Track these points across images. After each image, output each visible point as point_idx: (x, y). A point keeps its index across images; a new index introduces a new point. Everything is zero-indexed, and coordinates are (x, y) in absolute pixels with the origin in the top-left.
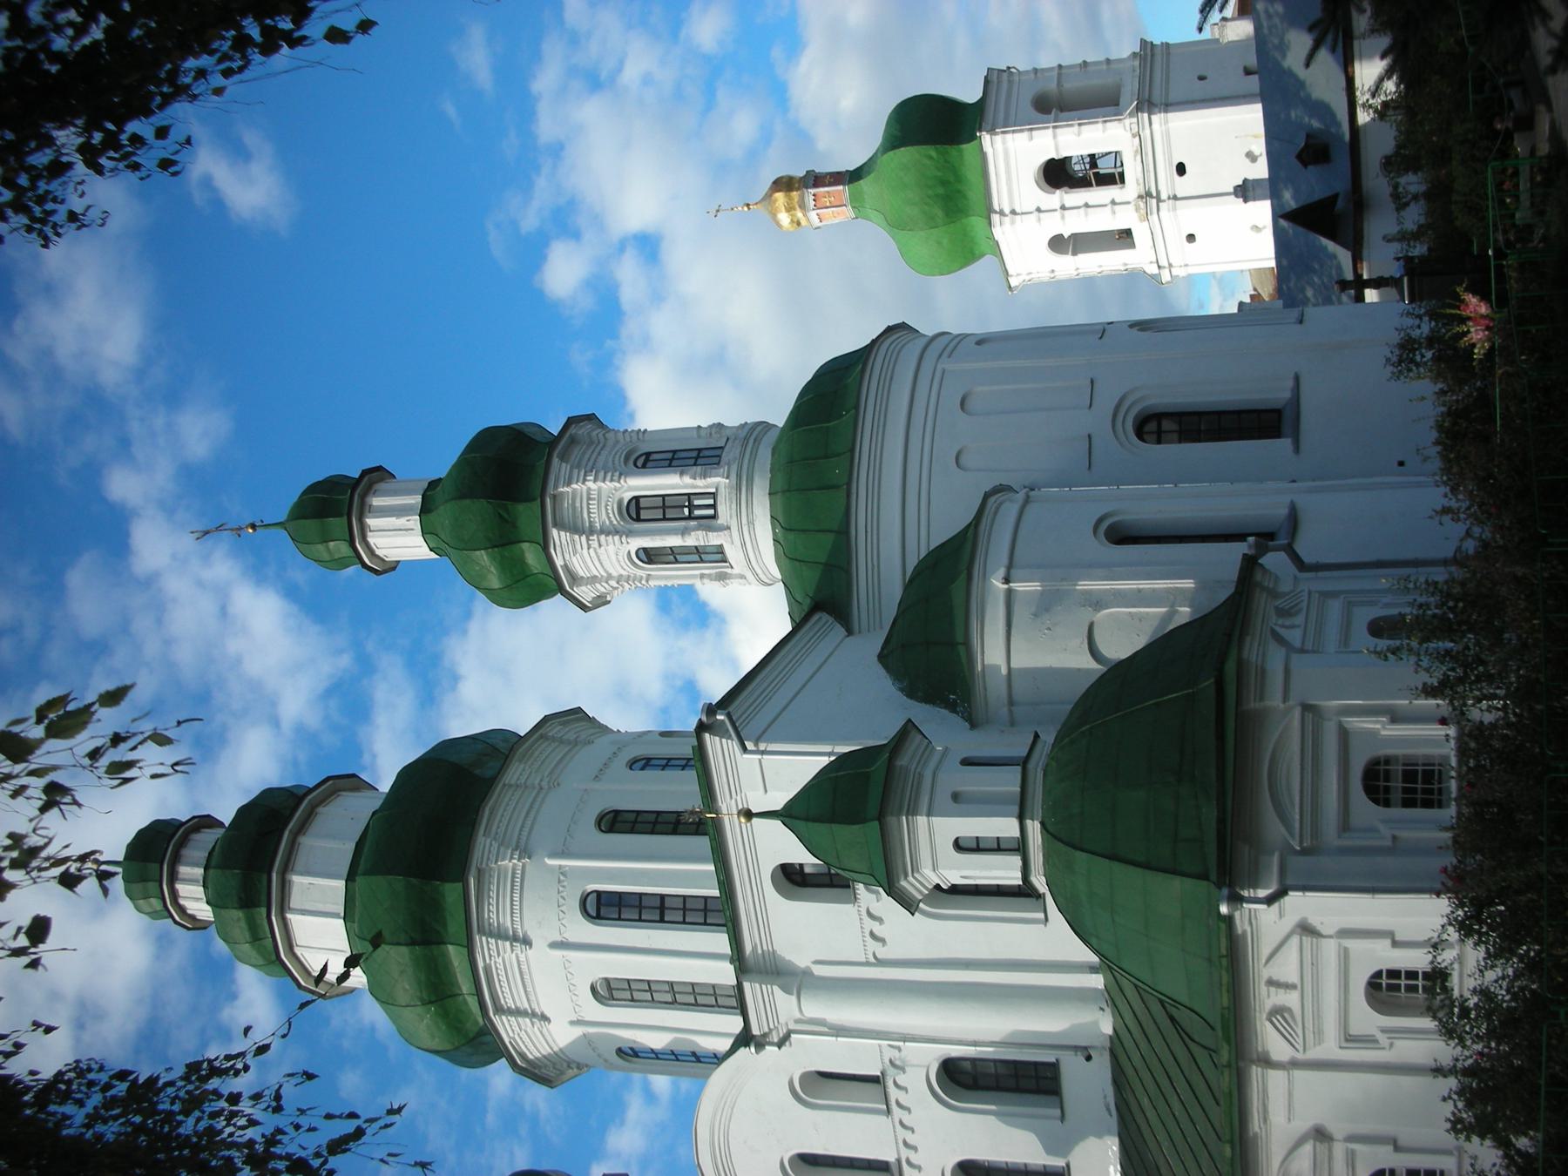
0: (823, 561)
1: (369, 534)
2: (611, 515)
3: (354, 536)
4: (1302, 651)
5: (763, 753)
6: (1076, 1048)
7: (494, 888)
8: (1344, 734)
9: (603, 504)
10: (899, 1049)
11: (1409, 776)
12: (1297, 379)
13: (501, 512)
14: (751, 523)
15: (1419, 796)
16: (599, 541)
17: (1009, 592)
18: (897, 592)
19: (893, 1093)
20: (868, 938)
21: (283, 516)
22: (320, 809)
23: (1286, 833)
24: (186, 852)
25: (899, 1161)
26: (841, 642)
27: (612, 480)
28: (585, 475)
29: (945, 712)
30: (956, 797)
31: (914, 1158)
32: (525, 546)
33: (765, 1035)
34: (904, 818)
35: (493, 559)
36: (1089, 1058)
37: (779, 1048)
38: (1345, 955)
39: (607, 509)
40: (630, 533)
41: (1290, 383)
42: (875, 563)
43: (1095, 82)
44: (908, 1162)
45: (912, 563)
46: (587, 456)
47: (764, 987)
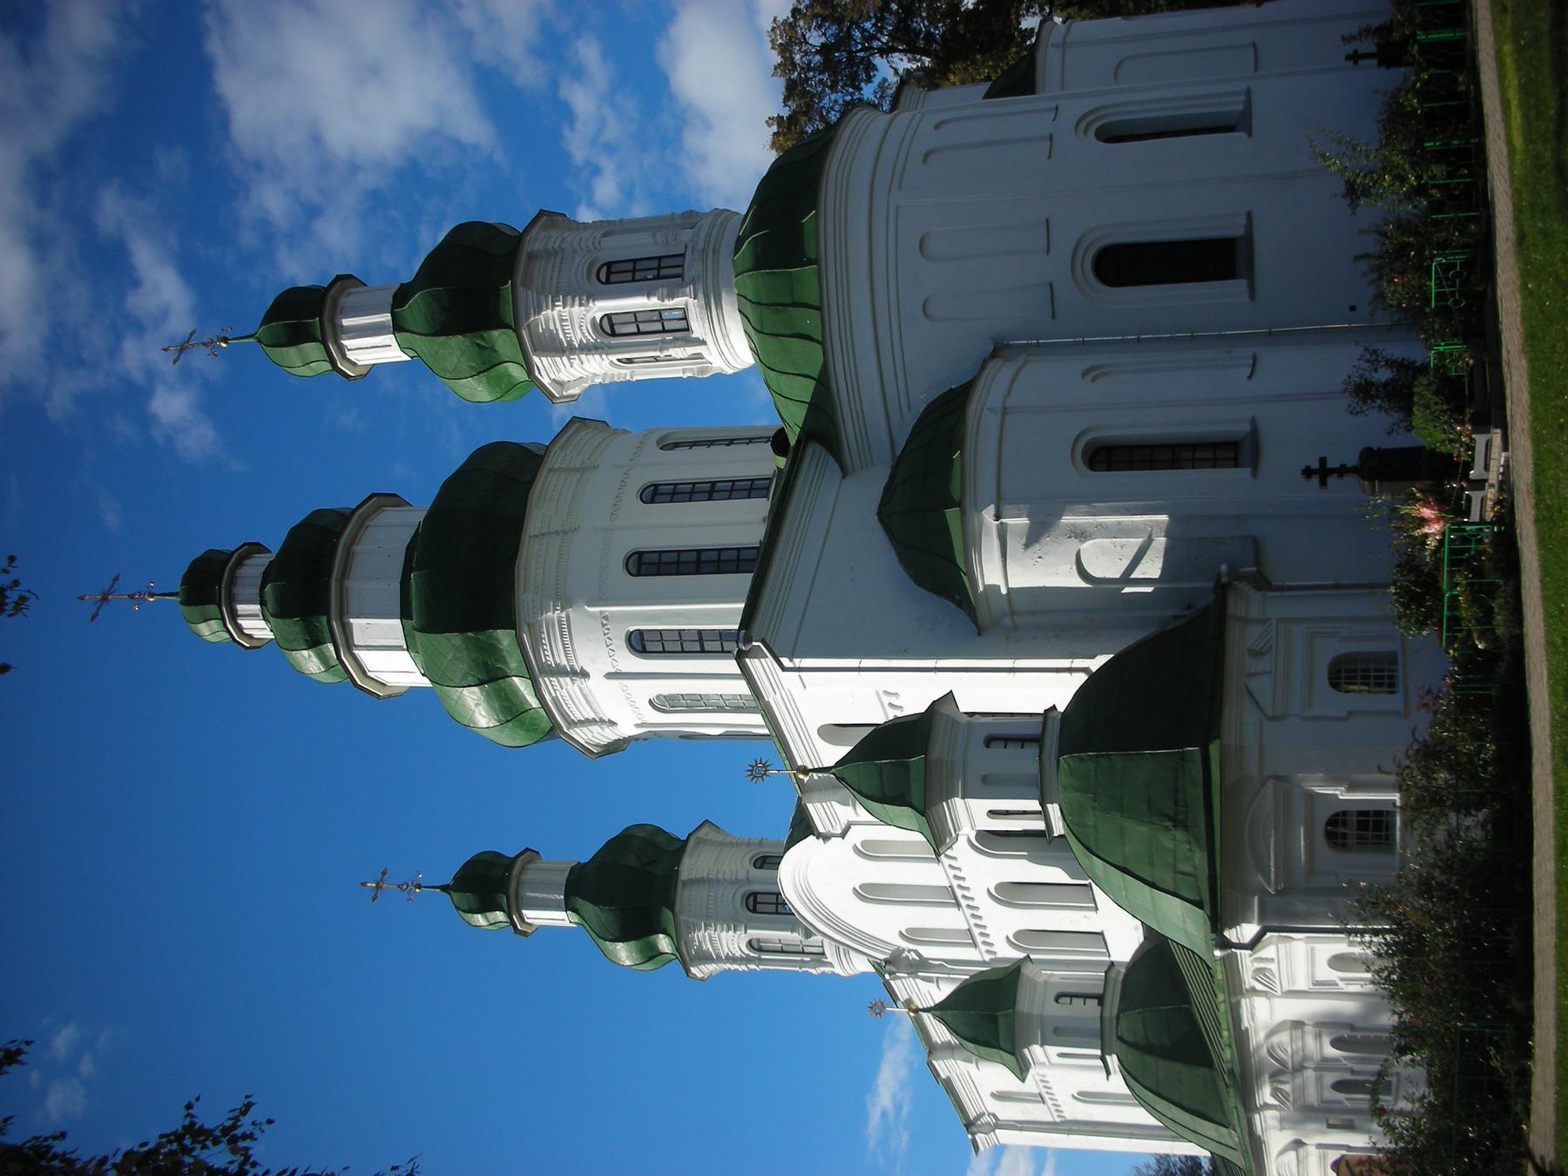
0: (808, 401)
1: (347, 353)
2: (587, 334)
4: (1273, 719)
7: (545, 636)
9: (577, 326)
13: (478, 342)
15: (1372, 681)
16: (580, 359)
22: (356, 548)
25: (951, 887)
26: (840, 488)
27: (581, 305)
28: (553, 302)
29: (953, 606)
34: (944, 803)
37: (843, 838)
39: (581, 330)
42: (860, 411)
46: (549, 276)
47: (824, 804)
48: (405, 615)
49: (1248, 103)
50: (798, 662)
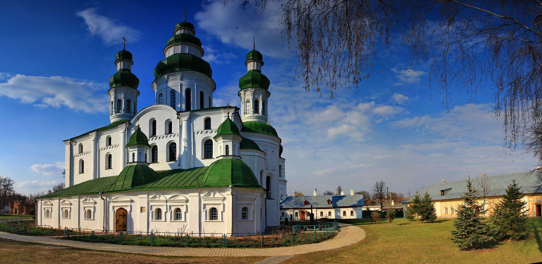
3: (253, 60)
5: (232, 117)
6: (180, 163)
8: (251, 204)
10: (178, 136)
11: (245, 214)
12: (274, 199)
14: (254, 118)
17: (255, 156)
18: (252, 140)
19: (169, 135)
20: (198, 131)
21: (256, 50)
23: (239, 195)
24: (189, 31)
30: (234, 146)
31: (157, 139)
32: (251, 84)
33: (179, 115)
35: (250, 79)
36: (178, 165)
38: (220, 204)
40: (253, 100)
41: (273, 198)
43: (282, 175)
44: (157, 138)
45: (256, 142)
48: (181, 53)
49: (272, 199)
50: (233, 117)
